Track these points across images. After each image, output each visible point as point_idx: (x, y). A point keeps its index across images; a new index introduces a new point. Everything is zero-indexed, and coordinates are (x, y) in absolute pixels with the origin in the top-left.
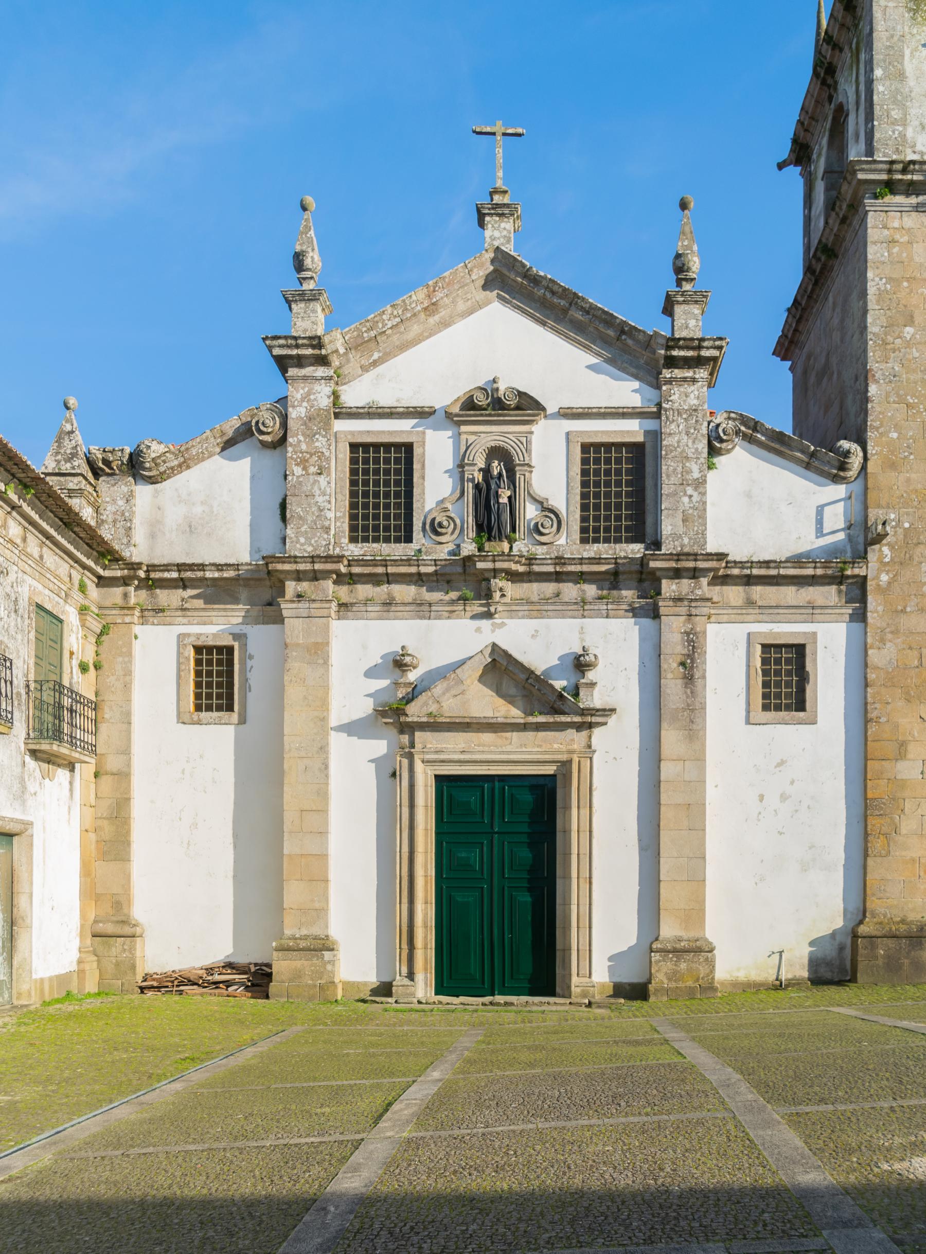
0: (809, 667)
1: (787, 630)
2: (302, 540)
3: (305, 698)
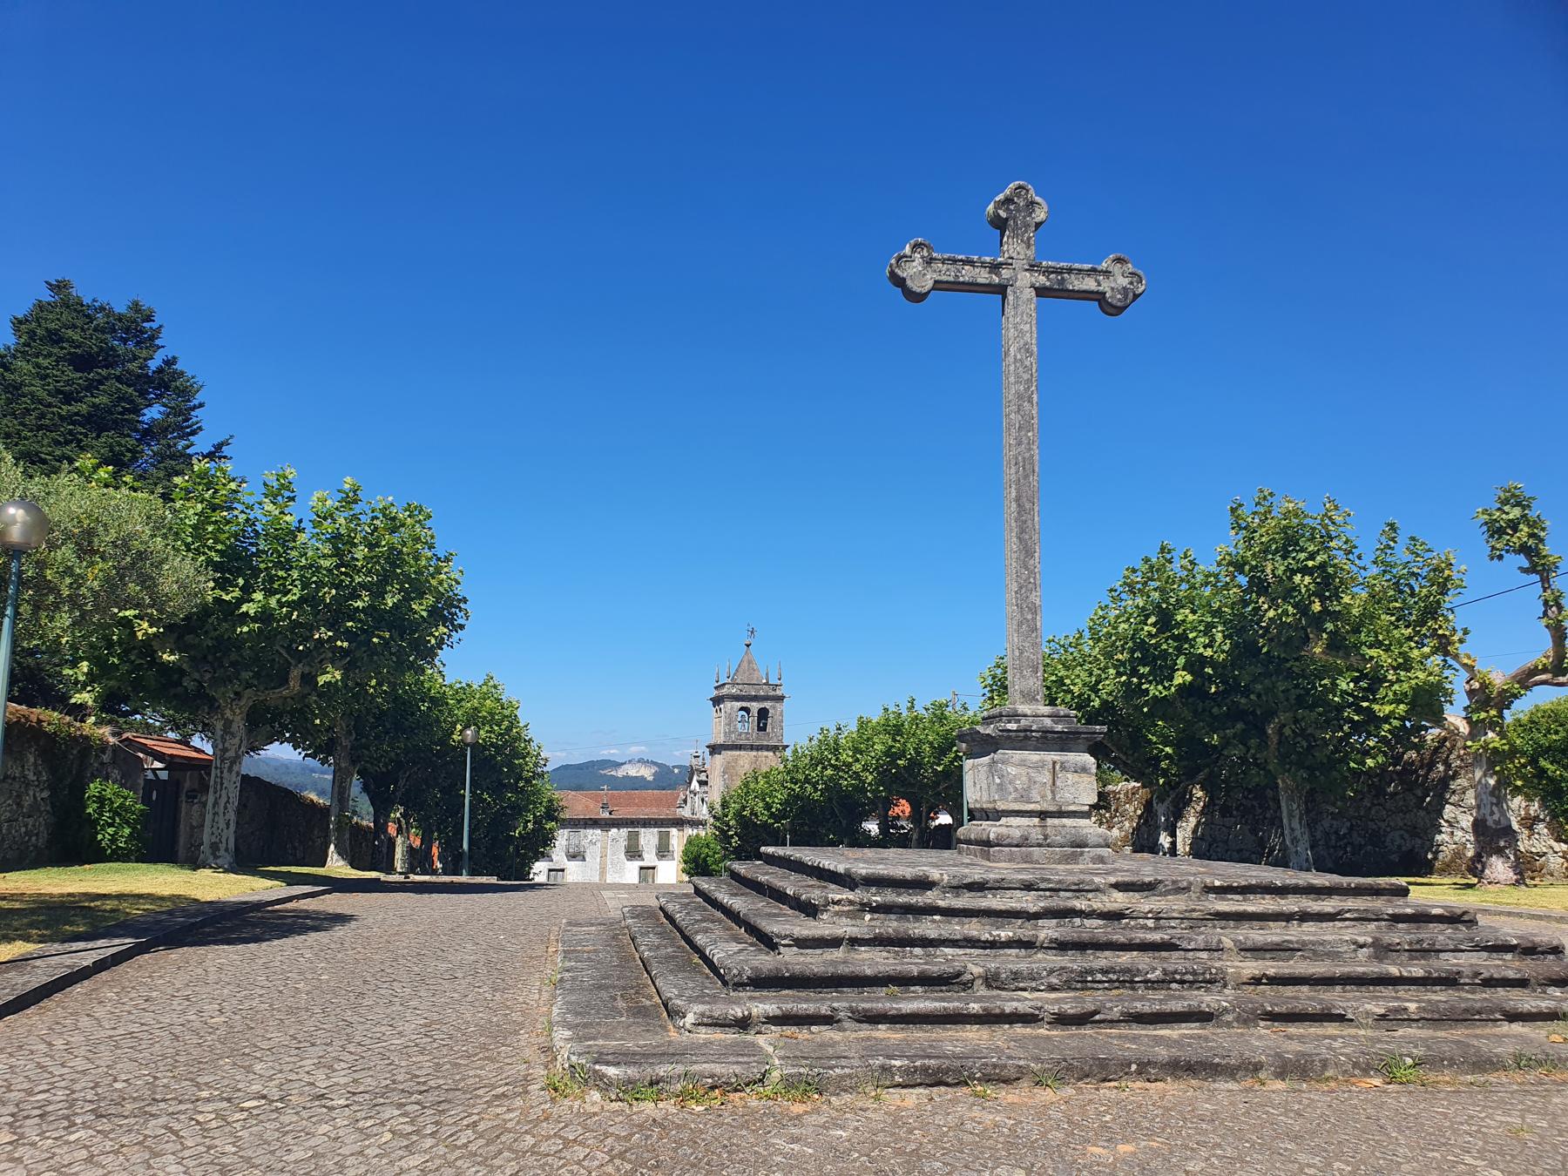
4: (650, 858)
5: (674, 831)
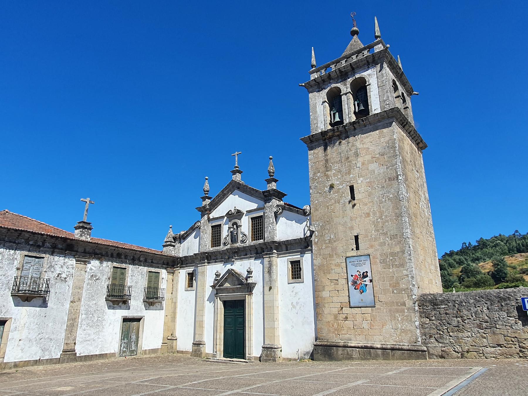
0: (301, 267)
1: (296, 257)
5: (163, 273)
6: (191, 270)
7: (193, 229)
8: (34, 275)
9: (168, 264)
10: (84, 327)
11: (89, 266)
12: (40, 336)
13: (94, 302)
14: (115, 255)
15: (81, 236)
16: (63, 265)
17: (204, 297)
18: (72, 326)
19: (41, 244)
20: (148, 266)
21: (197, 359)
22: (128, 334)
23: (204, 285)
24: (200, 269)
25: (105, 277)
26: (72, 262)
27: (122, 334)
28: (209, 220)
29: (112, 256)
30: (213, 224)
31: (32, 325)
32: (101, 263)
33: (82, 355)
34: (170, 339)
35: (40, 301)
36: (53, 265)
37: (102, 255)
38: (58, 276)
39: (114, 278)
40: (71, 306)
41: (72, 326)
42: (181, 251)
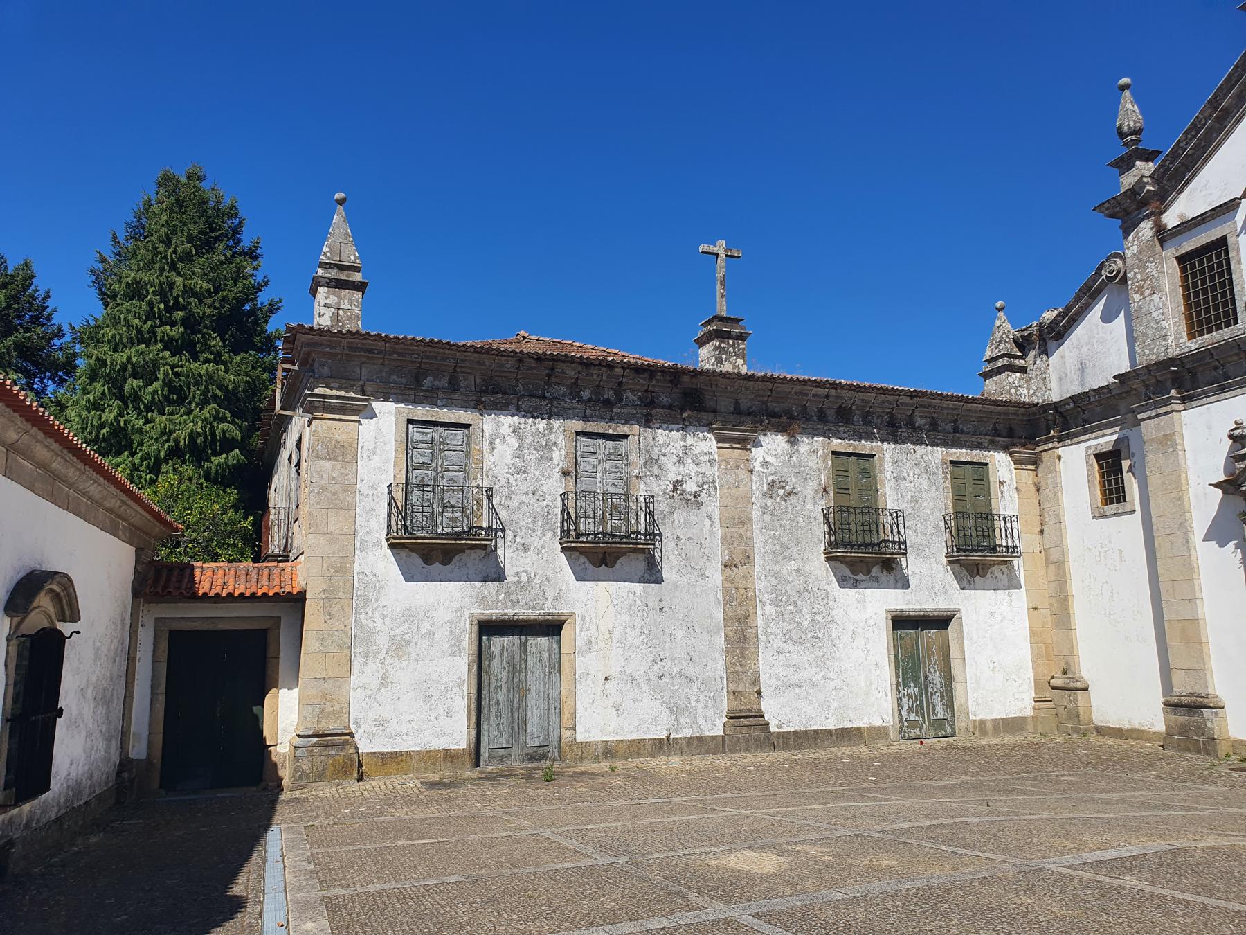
2: (1147, 352)
3: (1163, 483)
4: (929, 581)
5: (1001, 464)
6: (1106, 440)
7: (1089, 294)
8: (611, 490)
9: (1011, 433)
10: (777, 643)
11: (758, 454)
12: (656, 667)
13: (793, 565)
14: (830, 413)
15: (719, 361)
16: (681, 455)
17: (1184, 527)
18: (740, 640)
19: (610, 395)
20: (946, 444)
21: (1186, 761)
22: (915, 668)
23: (1177, 489)
24: (1150, 428)
25: (812, 485)
26: (705, 443)
27: (897, 669)
28: (1163, 236)
29: (822, 417)
30: (1188, 246)
31: (631, 635)
32: (793, 442)
33: (785, 729)
34: (1062, 687)
35: (638, 564)
36: (655, 457)
37: (792, 418)
38: (675, 489)
39: (841, 490)
40: (727, 579)
41: (740, 640)
42: (1054, 383)
